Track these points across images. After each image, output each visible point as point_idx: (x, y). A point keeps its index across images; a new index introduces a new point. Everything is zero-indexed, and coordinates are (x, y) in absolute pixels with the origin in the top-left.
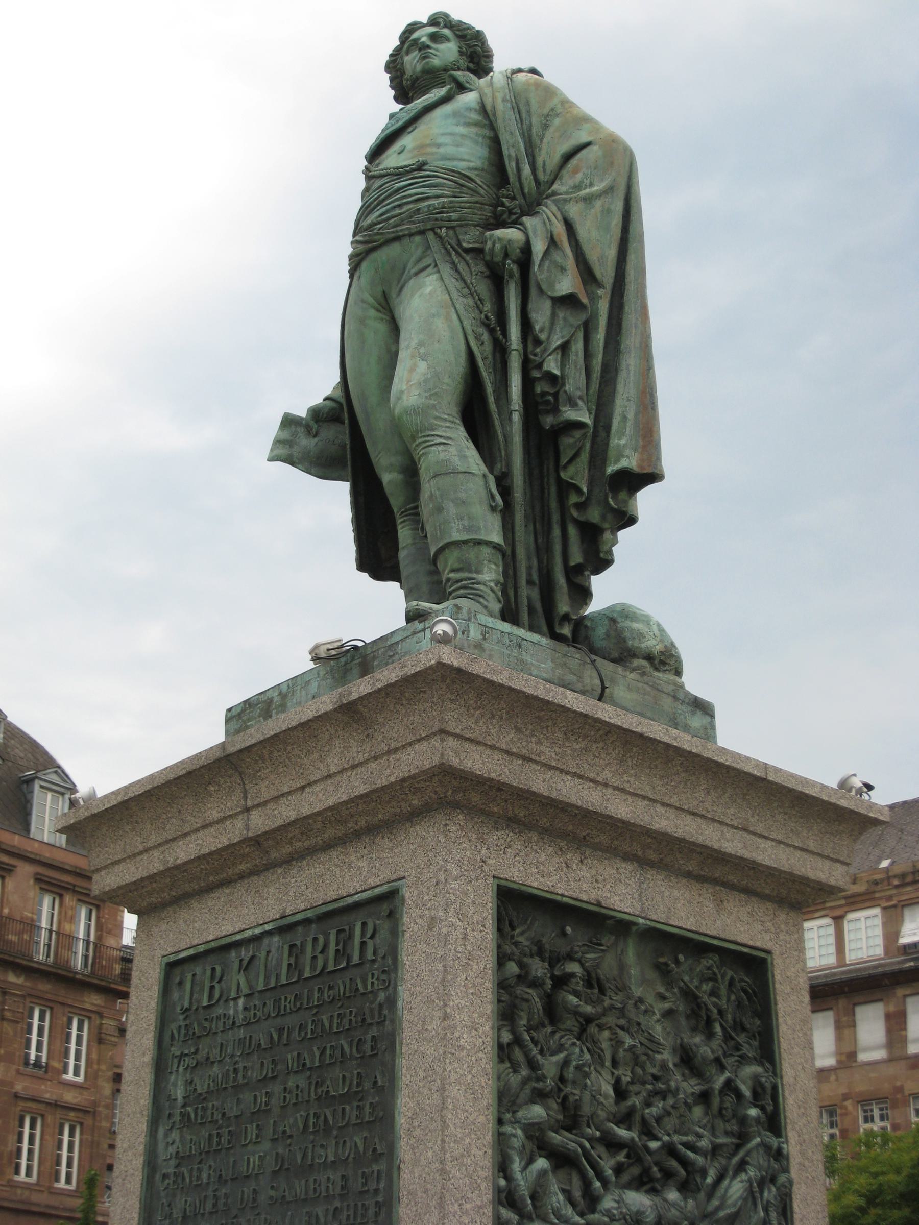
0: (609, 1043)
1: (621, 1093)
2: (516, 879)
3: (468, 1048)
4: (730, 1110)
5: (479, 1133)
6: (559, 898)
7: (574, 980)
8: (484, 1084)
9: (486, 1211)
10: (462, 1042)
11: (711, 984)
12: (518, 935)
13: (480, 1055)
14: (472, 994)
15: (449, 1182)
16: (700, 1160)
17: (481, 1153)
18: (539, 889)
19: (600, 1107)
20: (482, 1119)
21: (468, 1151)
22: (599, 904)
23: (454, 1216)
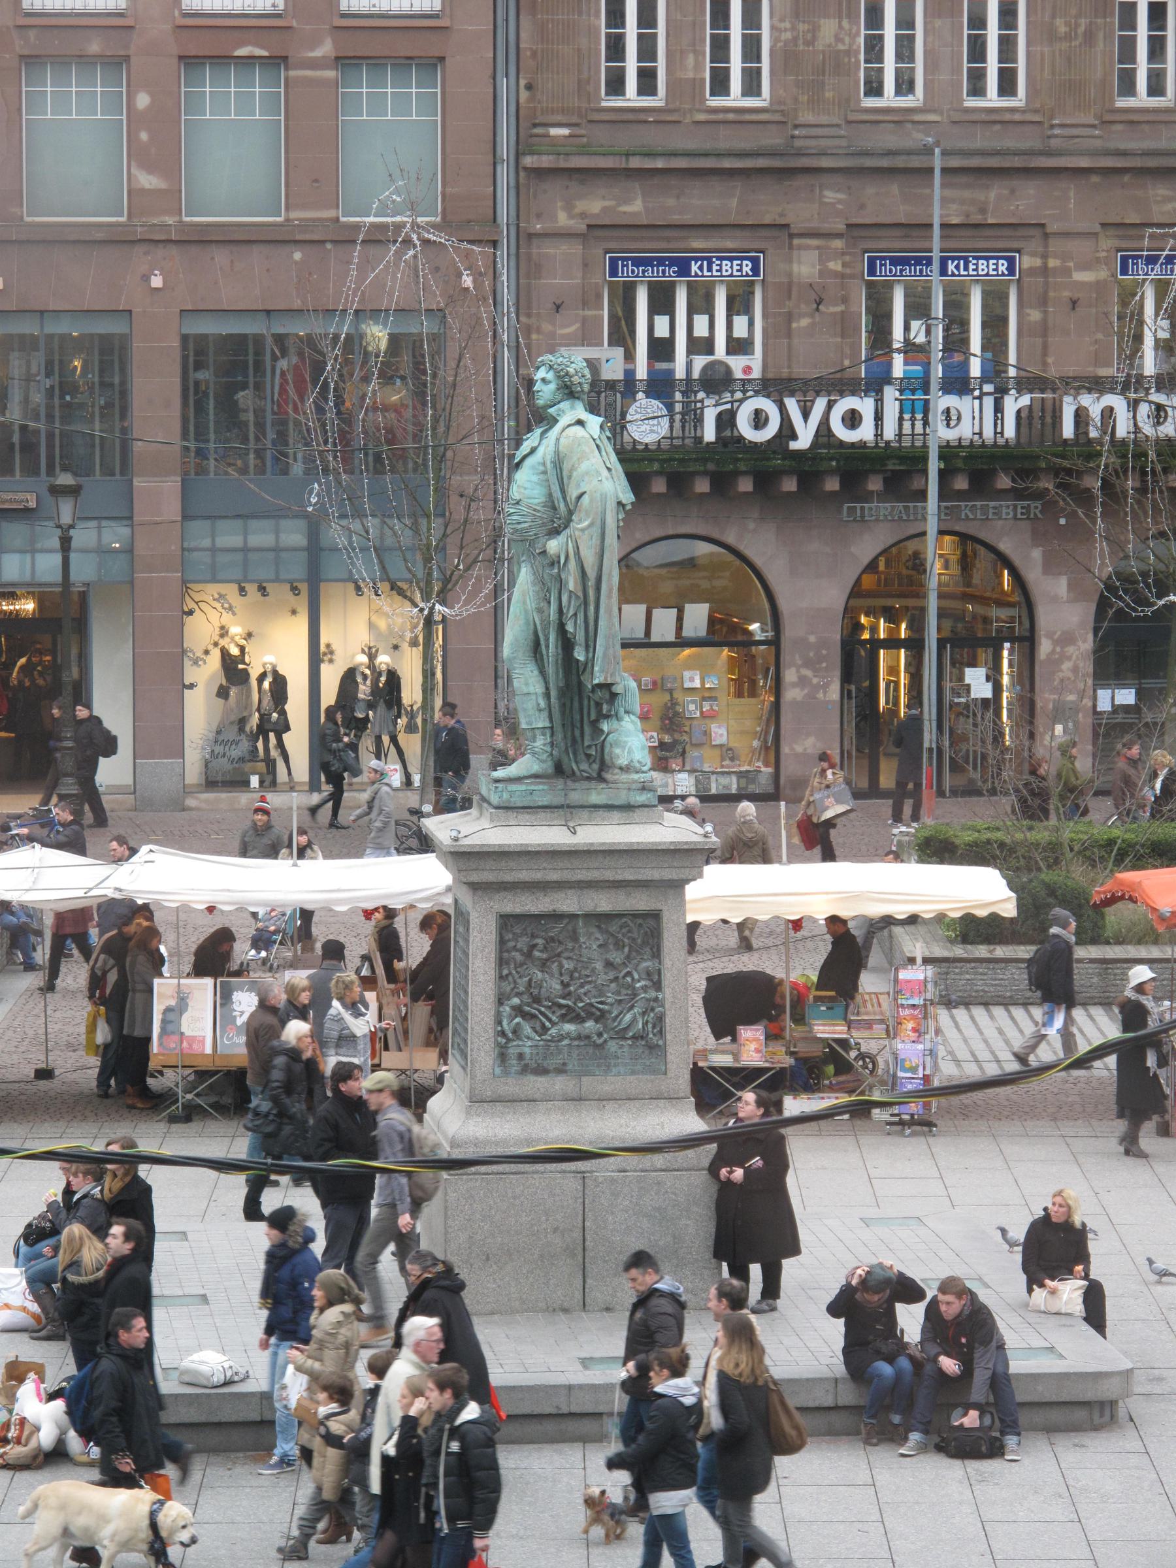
1: (565, 985)
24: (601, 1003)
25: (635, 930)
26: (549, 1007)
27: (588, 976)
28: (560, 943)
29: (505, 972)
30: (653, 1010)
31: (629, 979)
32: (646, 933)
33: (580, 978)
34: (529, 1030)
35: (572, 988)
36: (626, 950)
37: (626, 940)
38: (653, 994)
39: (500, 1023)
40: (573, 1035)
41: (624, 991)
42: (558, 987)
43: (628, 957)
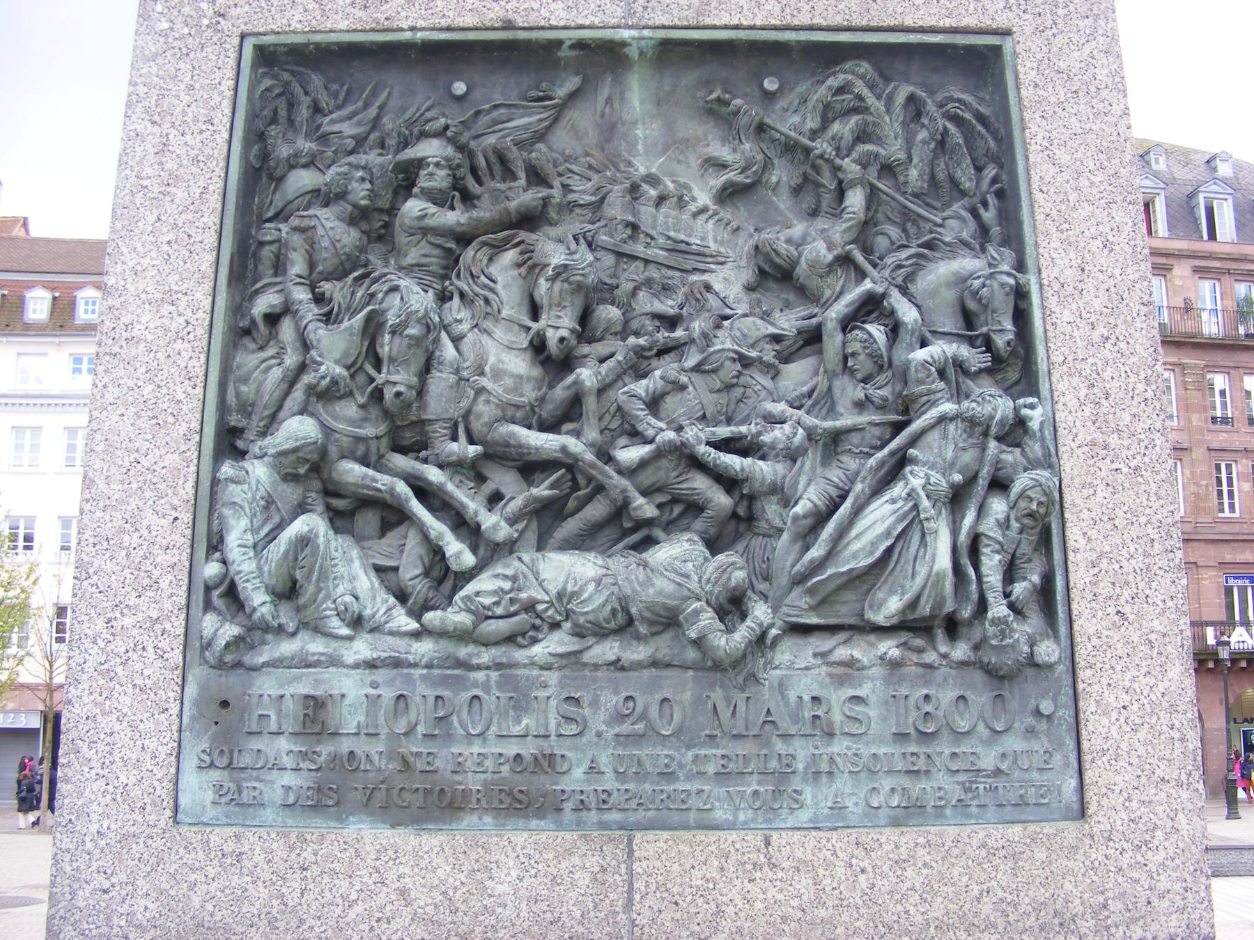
0: (515, 272)
2: (295, 25)
3: (150, 337)
4: (862, 357)
5: (162, 486)
6: (408, 35)
7: (423, 172)
8: (181, 396)
9: (168, 626)
10: (137, 331)
11: (854, 120)
12: (328, 124)
13: (179, 345)
14: (169, 242)
15: (86, 583)
16: (764, 470)
17: (165, 522)
18: (355, 31)
19: (483, 398)
20: (173, 460)
21: (133, 522)
22: (509, 26)
23: (95, 643)
24: (725, 445)
25: (891, 127)
26: (474, 472)
27: (672, 322)
28: (537, 177)
29: (264, 303)
30: (999, 485)
31: (877, 331)
32: (942, 143)
33: (624, 334)
34: (366, 582)
35: (587, 375)
36: (855, 200)
37: (850, 167)
38: (1001, 407)
39: (216, 544)
40: (593, 603)
41: (846, 390)
42: (519, 364)
43: (864, 233)
